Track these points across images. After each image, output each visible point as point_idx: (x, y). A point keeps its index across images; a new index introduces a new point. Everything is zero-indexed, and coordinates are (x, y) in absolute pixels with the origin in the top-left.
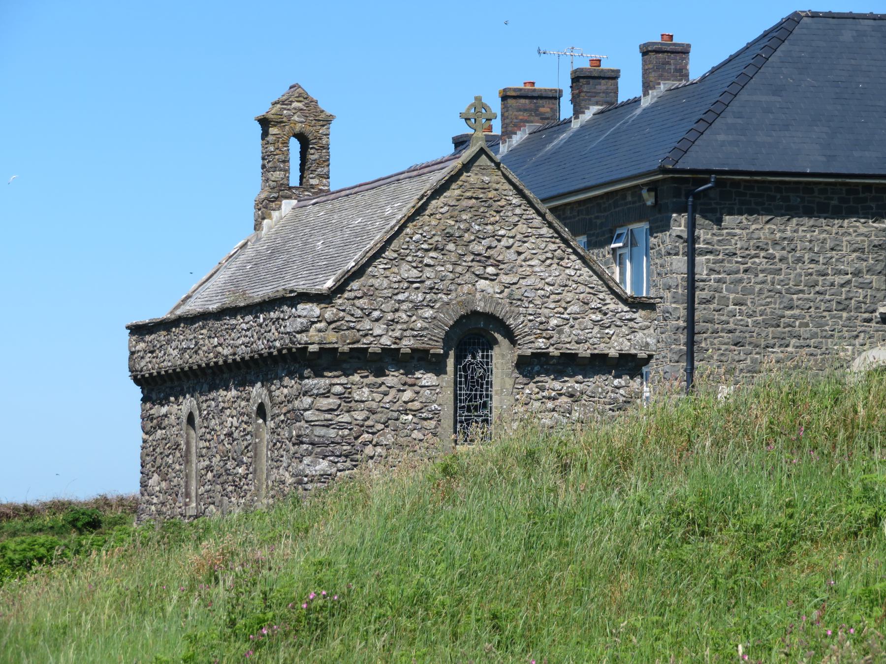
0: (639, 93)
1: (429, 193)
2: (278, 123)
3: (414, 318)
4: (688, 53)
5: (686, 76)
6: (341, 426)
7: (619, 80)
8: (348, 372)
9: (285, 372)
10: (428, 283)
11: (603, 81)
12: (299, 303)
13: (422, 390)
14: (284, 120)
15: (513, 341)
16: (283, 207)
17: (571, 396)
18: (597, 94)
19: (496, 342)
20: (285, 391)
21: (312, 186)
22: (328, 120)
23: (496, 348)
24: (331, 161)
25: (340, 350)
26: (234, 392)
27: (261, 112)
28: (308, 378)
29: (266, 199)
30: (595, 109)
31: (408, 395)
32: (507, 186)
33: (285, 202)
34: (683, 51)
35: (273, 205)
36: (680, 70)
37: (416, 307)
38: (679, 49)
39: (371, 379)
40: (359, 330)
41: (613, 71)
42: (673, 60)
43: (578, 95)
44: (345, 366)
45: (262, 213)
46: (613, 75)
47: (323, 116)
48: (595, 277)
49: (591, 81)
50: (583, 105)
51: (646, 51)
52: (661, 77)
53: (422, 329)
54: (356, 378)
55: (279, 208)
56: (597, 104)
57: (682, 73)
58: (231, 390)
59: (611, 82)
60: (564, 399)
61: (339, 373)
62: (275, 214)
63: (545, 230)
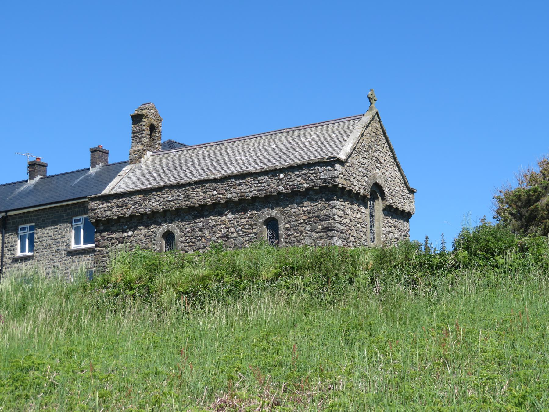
0: (88, 165)
1: (366, 126)
2: (146, 117)
3: (363, 180)
4: (108, 153)
5: (107, 162)
6: (344, 225)
7: (47, 167)
8: (345, 200)
9: (306, 199)
10: (366, 166)
11: (42, 167)
12: (335, 164)
13: (362, 214)
14: (148, 116)
15: (383, 198)
16: (148, 154)
17: (395, 227)
18: (39, 171)
19: (377, 198)
20: (305, 209)
21: (156, 148)
22: (161, 121)
23: (376, 201)
24: (162, 138)
25: (347, 189)
26: (230, 216)
27: (134, 113)
28: (335, 200)
29: (143, 149)
30: (39, 177)
31: (359, 215)
32: (381, 130)
33: (148, 152)
34: (106, 153)
35: (145, 152)
36: (106, 160)
37: (363, 176)
38: (106, 152)
39: (350, 205)
40: (351, 181)
41: (46, 164)
42: (106, 154)
43: (34, 171)
44: (344, 197)
45: (139, 155)
46: (45, 165)
47: (159, 118)
48: (401, 177)
49: (39, 166)
50: (36, 174)
51: (93, 151)
52: (100, 161)
53: (365, 186)
54: (346, 203)
55: (146, 155)
56: (40, 175)
57: (106, 161)
58: (226, 215)
59: (45, 168)
60: (393, 228)
61: (342, 200)
62: (145, 157)
63: (390, 153)
